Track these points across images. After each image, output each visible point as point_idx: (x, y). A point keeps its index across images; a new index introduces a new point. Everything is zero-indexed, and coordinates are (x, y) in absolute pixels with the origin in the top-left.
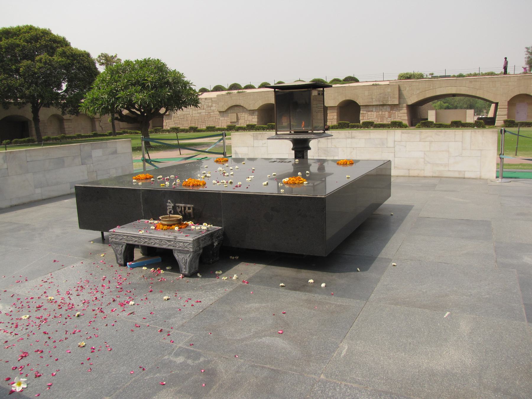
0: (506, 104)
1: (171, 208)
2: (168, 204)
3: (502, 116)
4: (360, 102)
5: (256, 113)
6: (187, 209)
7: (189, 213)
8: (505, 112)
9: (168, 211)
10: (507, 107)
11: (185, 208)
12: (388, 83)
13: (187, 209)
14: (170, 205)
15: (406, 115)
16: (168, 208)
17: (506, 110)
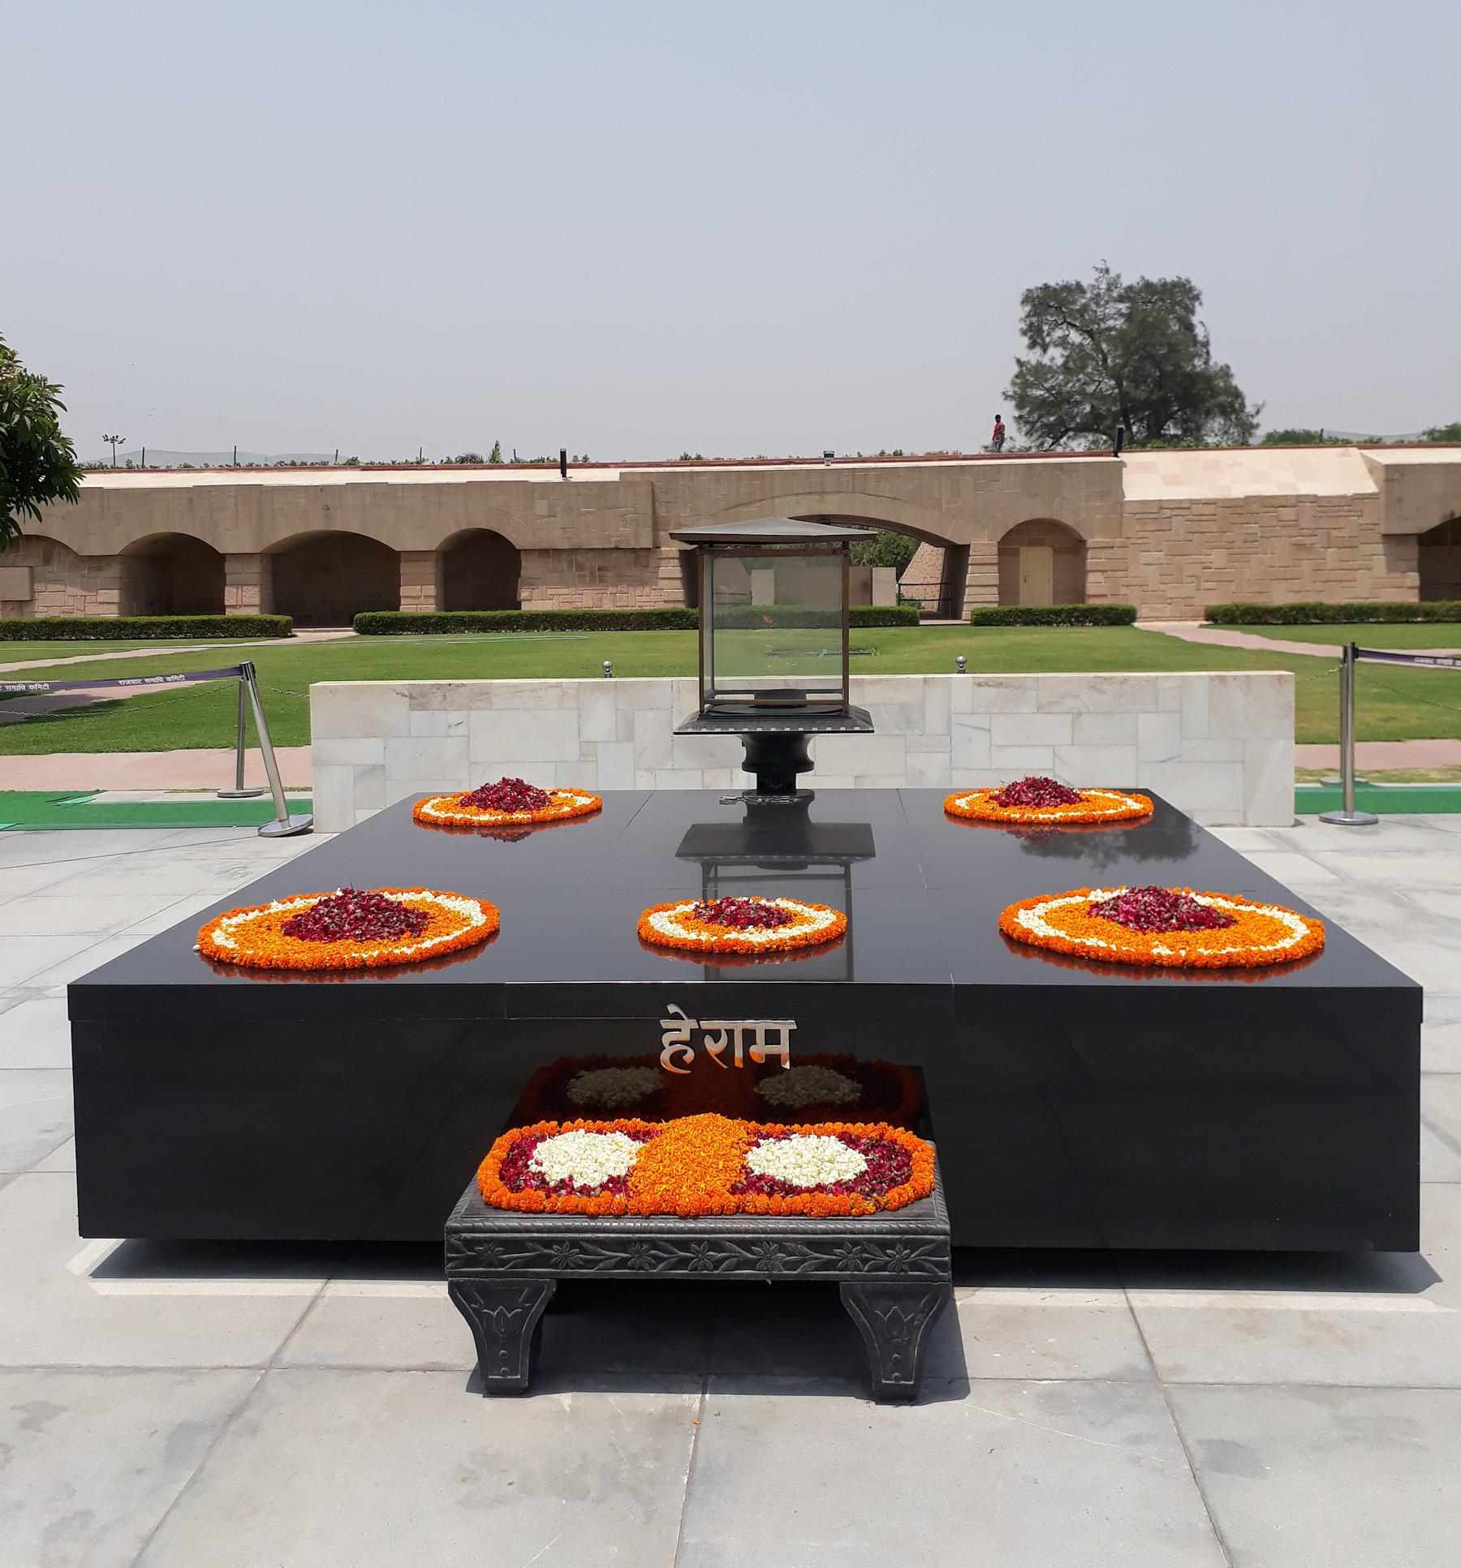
0: (995, 551)
1: (685, 1035)
2: (665, 1024)
3: (982, 590)
4: (518, 540)
5: (114, 571)
6: (760, 1037)
7: (774, 1060)
8: (992, 576)
9: (665, 1056)
10: (995, 559)
11: (749, 1037)
12: (613, 475)
13: (760, 1037)
14: (677, 1031)
15: (678, 584)
16: (666, 1039)
17: (996, 568)
